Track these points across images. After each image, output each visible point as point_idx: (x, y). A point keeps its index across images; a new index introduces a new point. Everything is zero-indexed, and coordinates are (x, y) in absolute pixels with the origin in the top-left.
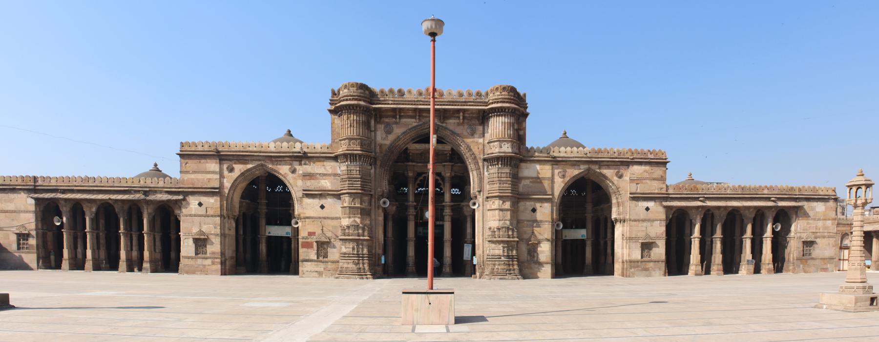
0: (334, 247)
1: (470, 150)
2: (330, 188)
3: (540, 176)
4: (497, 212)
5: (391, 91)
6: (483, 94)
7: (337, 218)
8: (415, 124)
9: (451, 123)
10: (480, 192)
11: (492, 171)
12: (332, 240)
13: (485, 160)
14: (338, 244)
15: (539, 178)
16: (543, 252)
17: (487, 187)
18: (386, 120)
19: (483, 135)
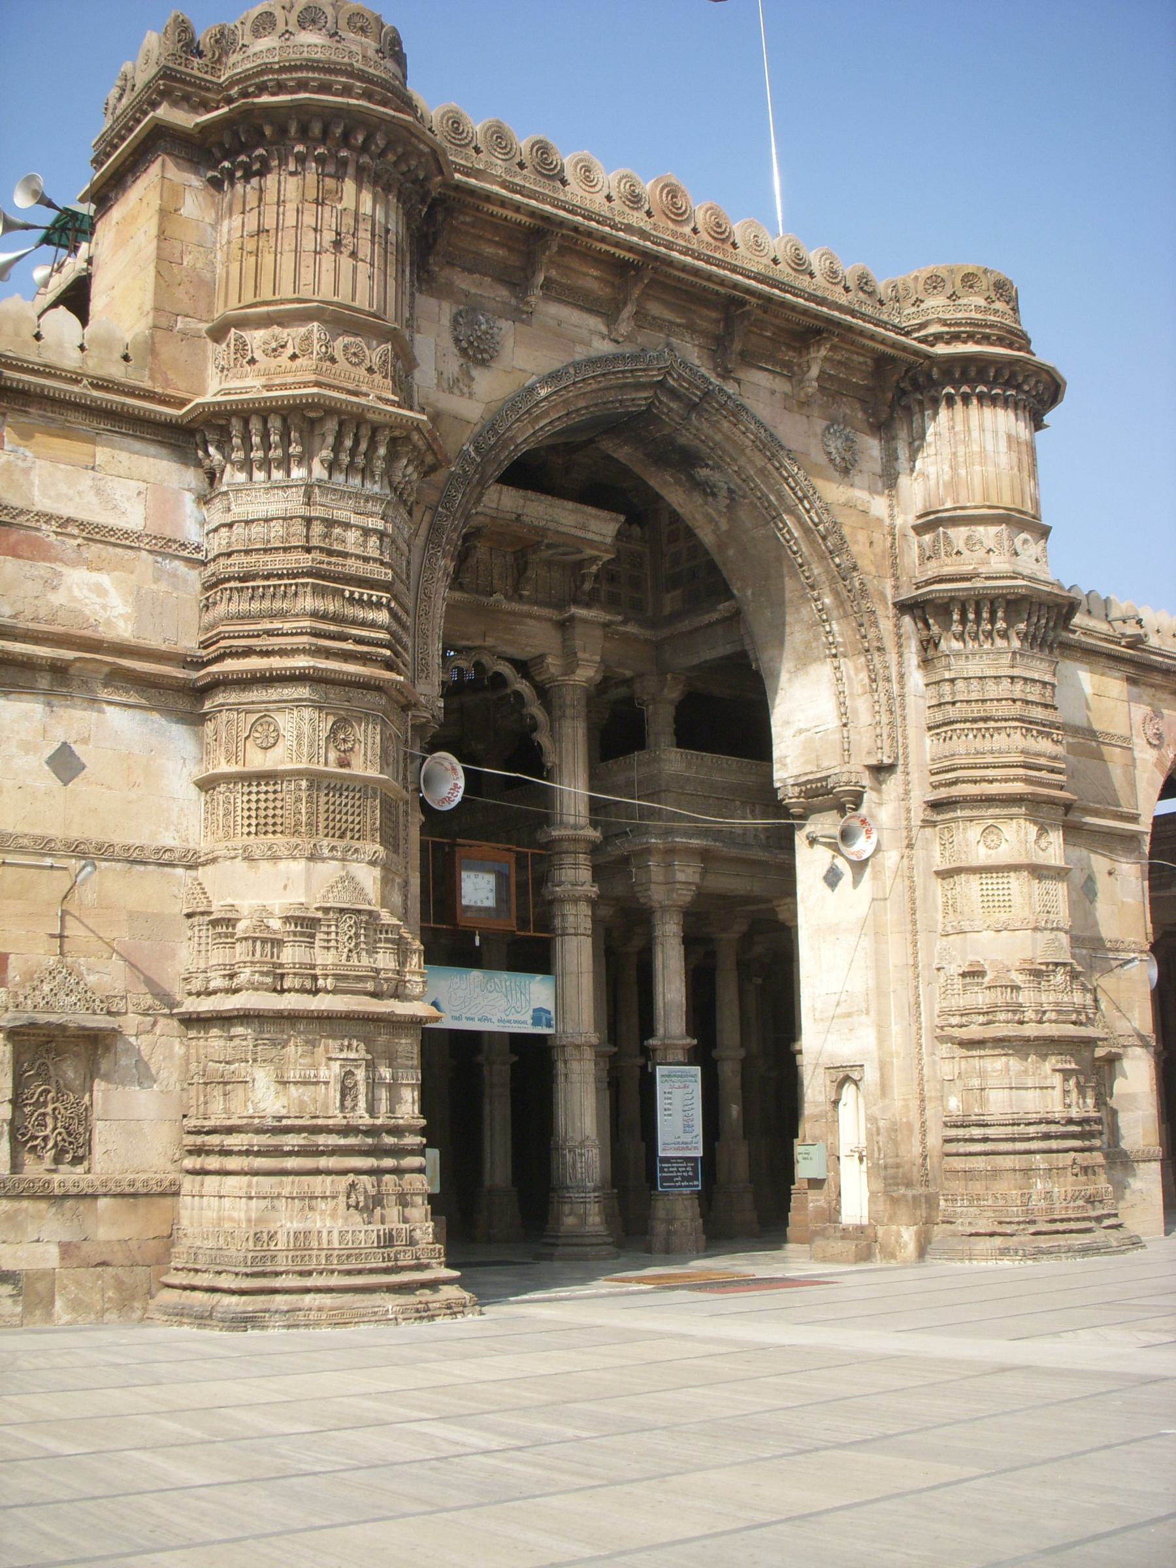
0: (144, 1075)
1: (841, 547)
2: (123, 630)
3: (1096, 727)
4: (1017, 884)
5: (499, 137)
6: (882, 286)
7: (164, 860)
8: (604, 347)
9: (760, 391)
10: (880, 771)
11: (973, 668)
12: (130, 1023)
13: (903, 607)
14: (163, 1048)
15: (1091, 733)
16: (1131, 1098)
17: (923, 749)
18: (463, 282)
19: (889, 479)
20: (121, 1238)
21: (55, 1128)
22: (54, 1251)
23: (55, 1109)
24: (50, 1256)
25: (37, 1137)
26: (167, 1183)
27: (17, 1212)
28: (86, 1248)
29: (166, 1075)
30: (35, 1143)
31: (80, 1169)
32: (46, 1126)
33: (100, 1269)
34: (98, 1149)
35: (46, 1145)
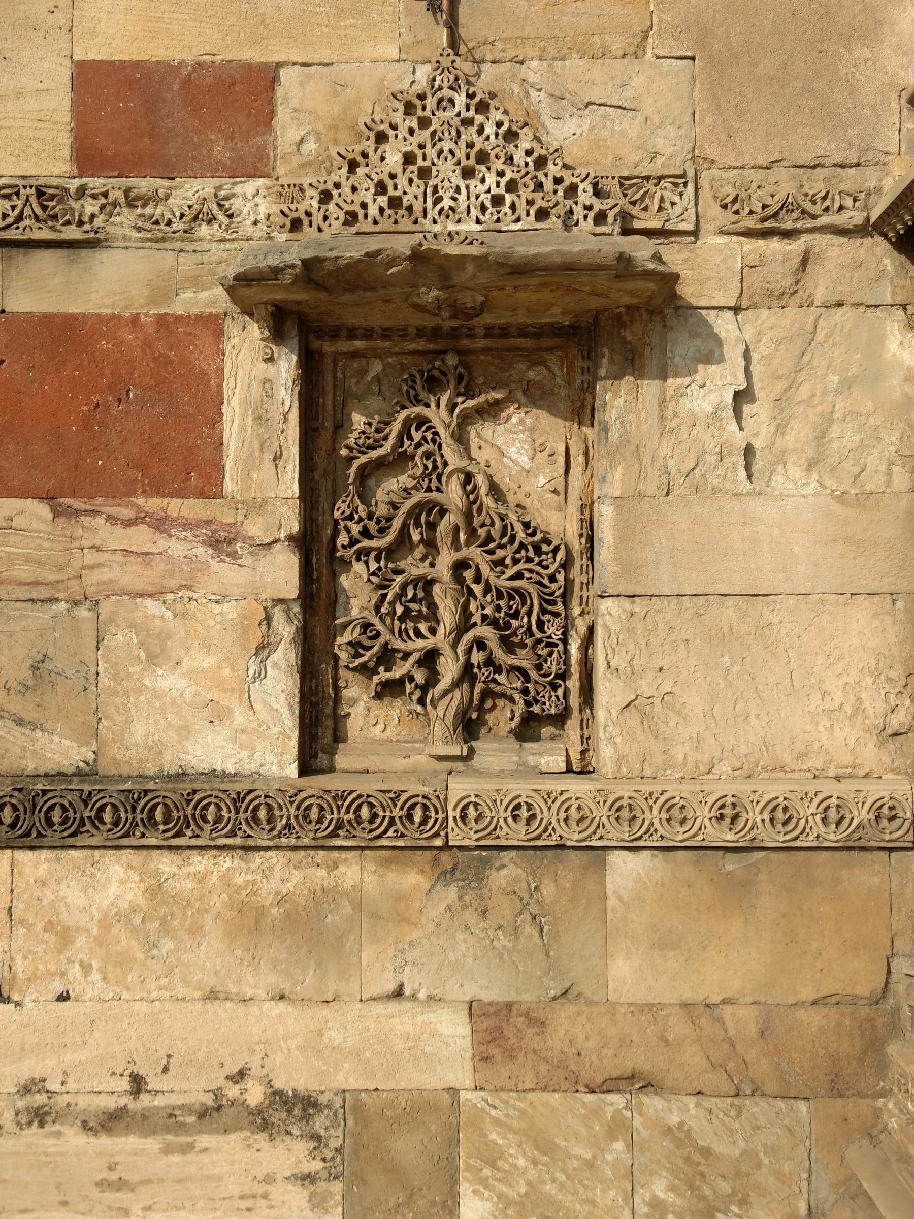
20: (689, 995)
21: (464, 624)
22: (454, 1029)
23: (460, 566)
24: (437, 1047)
25: (406, 655)
26: (863, 815)
27: (326, 897)
28: (567, 1027)
29: (852, 439)
30: (397, 673)
31: (549, 755)
32: (433, 617)
33: (617, 1100)
34: (607, 692)
35: (433, 678)
